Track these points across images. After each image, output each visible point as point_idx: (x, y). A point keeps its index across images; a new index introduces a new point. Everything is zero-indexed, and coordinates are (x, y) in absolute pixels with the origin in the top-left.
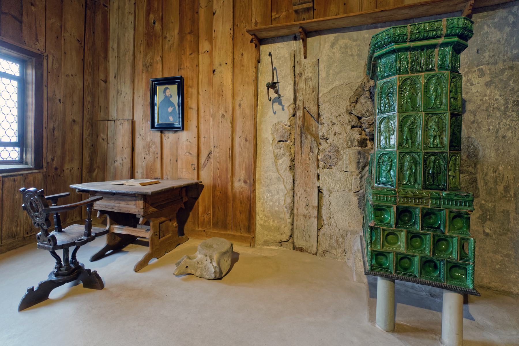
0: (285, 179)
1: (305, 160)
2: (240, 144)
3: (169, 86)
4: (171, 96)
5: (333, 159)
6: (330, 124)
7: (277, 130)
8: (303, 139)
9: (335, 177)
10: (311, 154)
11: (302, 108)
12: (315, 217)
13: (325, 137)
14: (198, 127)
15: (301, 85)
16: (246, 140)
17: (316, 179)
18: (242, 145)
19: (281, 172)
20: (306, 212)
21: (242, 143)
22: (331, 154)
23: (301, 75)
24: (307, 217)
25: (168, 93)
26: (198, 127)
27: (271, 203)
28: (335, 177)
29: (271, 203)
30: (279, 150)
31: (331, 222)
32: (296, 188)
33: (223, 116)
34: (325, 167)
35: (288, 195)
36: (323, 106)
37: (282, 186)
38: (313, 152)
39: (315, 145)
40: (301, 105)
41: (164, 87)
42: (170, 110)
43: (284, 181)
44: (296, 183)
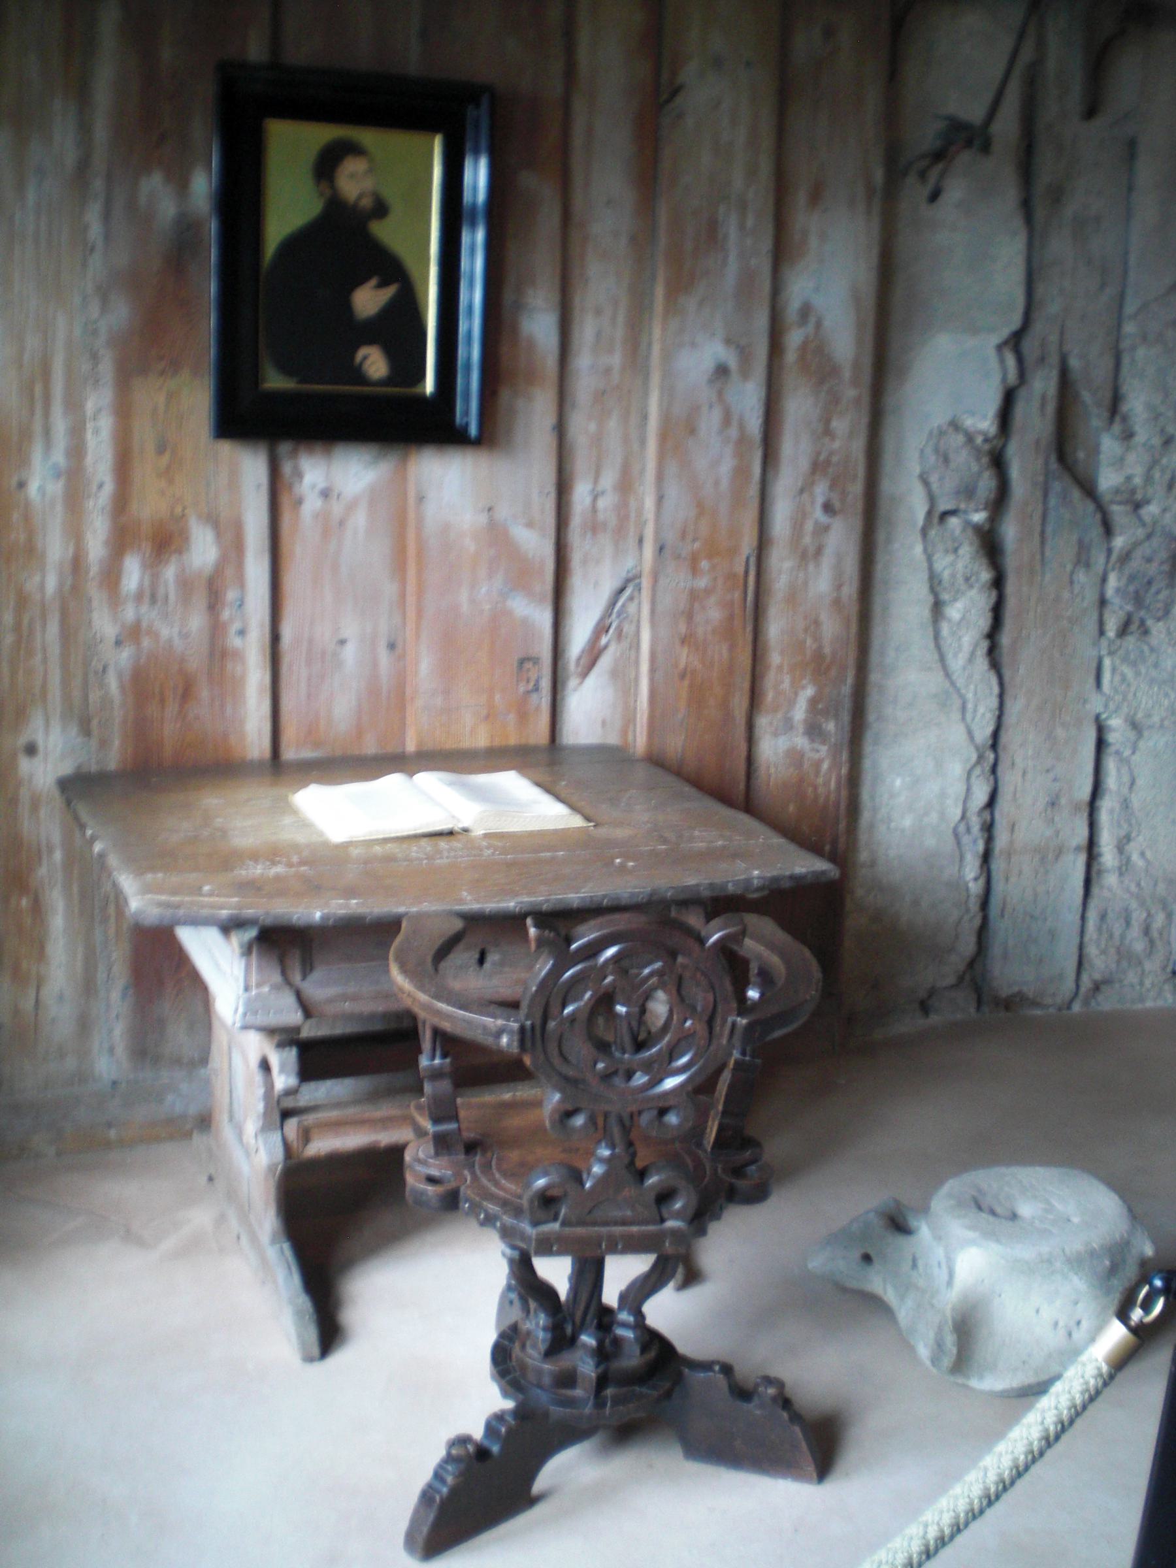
0: (970, 696)
1: (1057, 599)
2: (797, 525)
3: (367, 137)
4: (381, 209)
5: (1158, 593)
6: (1157, 441)
7: (946, 460)
8: (1053, 502)
9: (1156, 665)
10: (1081, 577)
11: (1054, 360)
12: (1078, 849)
13: (1139, 496)
14: (560, 429)
15: (1060, 246)
16: (828, 508)
17: (1091, 680)
18: (807, 540)
19: (957, 663)
20: (1049, 833)
21: (809, 526)
22: (1153, 569)
23: (1057, 195)
24: (1049, 854)
25: (353, 181)
26: (560, 429)
27: (907, 822)
28: (1156, 665)
29: (907, 822)
30: (950, 558)
31: (1129, 859)
32: (1004, 738)
33: (722, 371)
34: (1123, 631)
35: (977, 771)
36: (1141, 352)
37: (956, 734)
38: (1088, 565)
39: (1096, 532)
40: (1054, 338)
41: (319, 134)
42: (368, 300)
43: (964, 709)
44: (1014, 708)
